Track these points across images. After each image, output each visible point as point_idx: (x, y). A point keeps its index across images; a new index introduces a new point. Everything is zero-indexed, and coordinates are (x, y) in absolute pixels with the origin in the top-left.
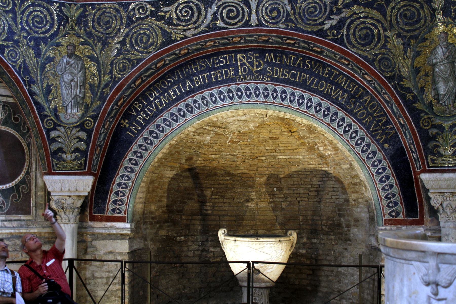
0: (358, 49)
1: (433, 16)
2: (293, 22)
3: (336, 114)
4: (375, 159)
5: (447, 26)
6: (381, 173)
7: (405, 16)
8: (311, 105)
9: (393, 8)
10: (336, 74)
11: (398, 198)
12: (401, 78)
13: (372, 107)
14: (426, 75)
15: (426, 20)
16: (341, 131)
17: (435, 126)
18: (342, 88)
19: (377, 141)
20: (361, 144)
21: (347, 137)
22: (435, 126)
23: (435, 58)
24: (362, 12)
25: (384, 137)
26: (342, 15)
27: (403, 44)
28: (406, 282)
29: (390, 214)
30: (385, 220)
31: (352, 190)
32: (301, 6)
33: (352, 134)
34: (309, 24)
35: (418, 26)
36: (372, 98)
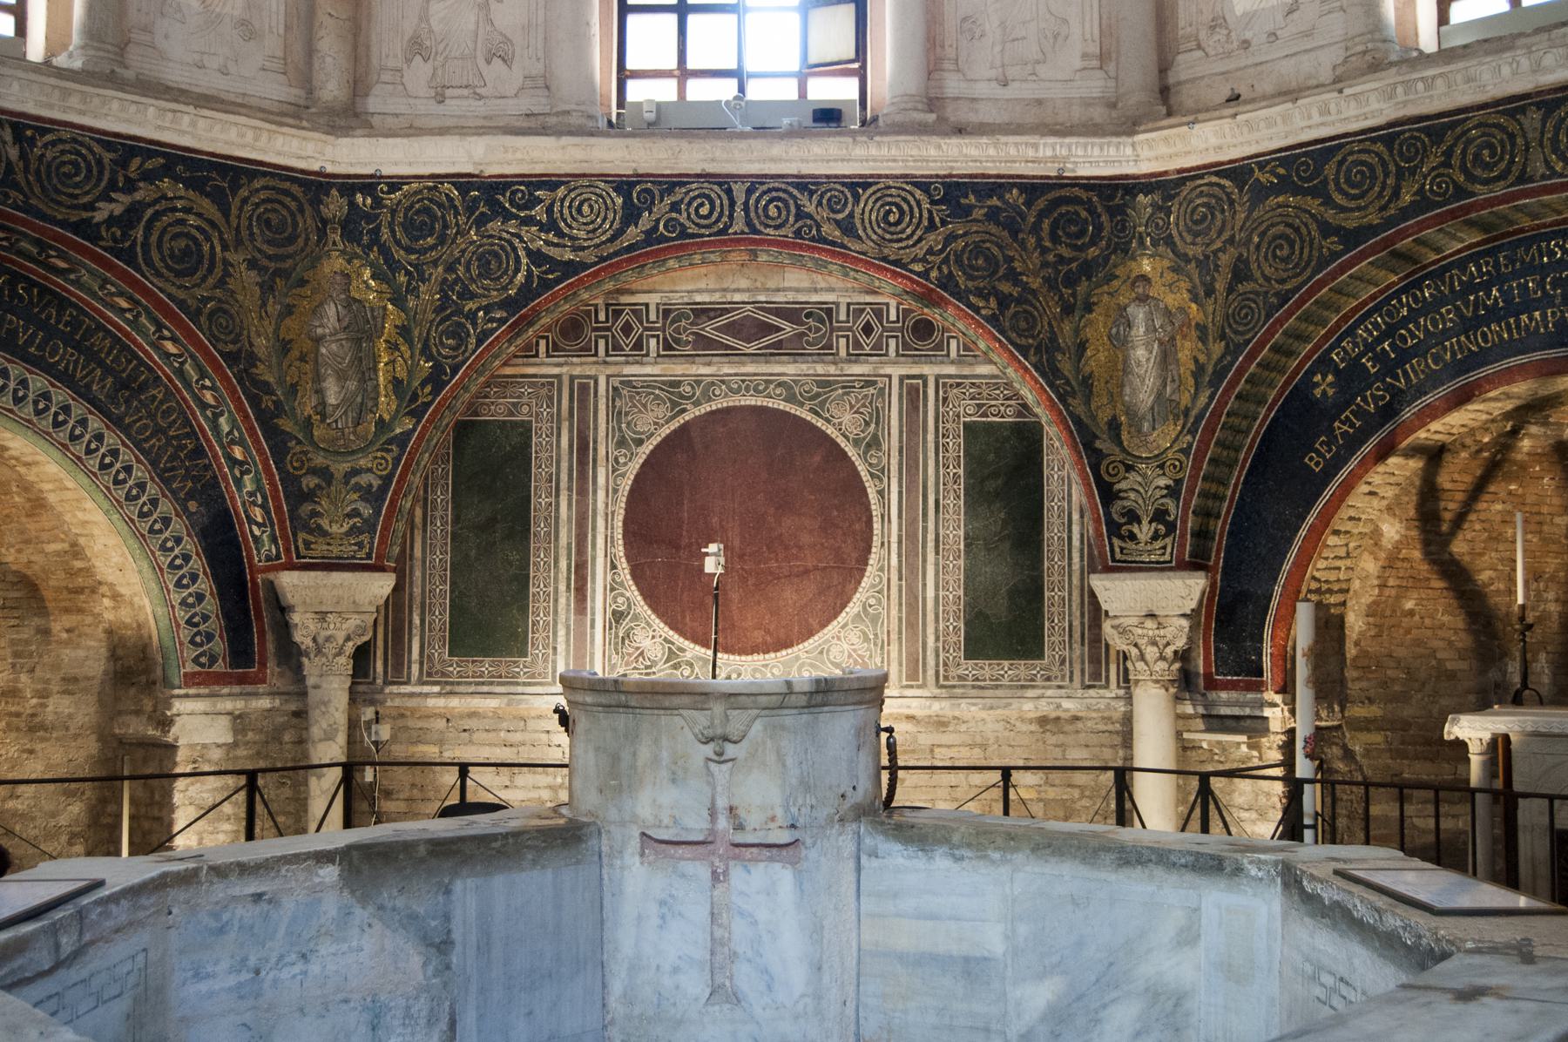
0: (167, 280)
1: (322, 234)
2: (21, 191)
3: (83, 422)
4: (167, 534)
5: (349, 262)
6: (180, 567)
7: (268, 222)
8: (25, 397)
9: (245, 201)
10: (89, 327)
11: (214, 624)
12: (252, 359)
13: (167, 413)
14: (302, 359)
15: (307, 239)
16: (93, 464)
17: (314, 471)
18: (101, 363)
19: (173, 492)
20: (137, 497)
21: (108, 479)
22: (314, 471)
23: (322, 326)
24: (181, 198)
25: (190, 484)
26: (138, 196)
27: (261, 285)
28: (664, 741)
29: (196, 660)
30: (186, 675)
31: (67, 604)
32: (43, 155)
33: (118, 472)
34: (59, 203)
35: (291, 249)
36: (168, 393)
